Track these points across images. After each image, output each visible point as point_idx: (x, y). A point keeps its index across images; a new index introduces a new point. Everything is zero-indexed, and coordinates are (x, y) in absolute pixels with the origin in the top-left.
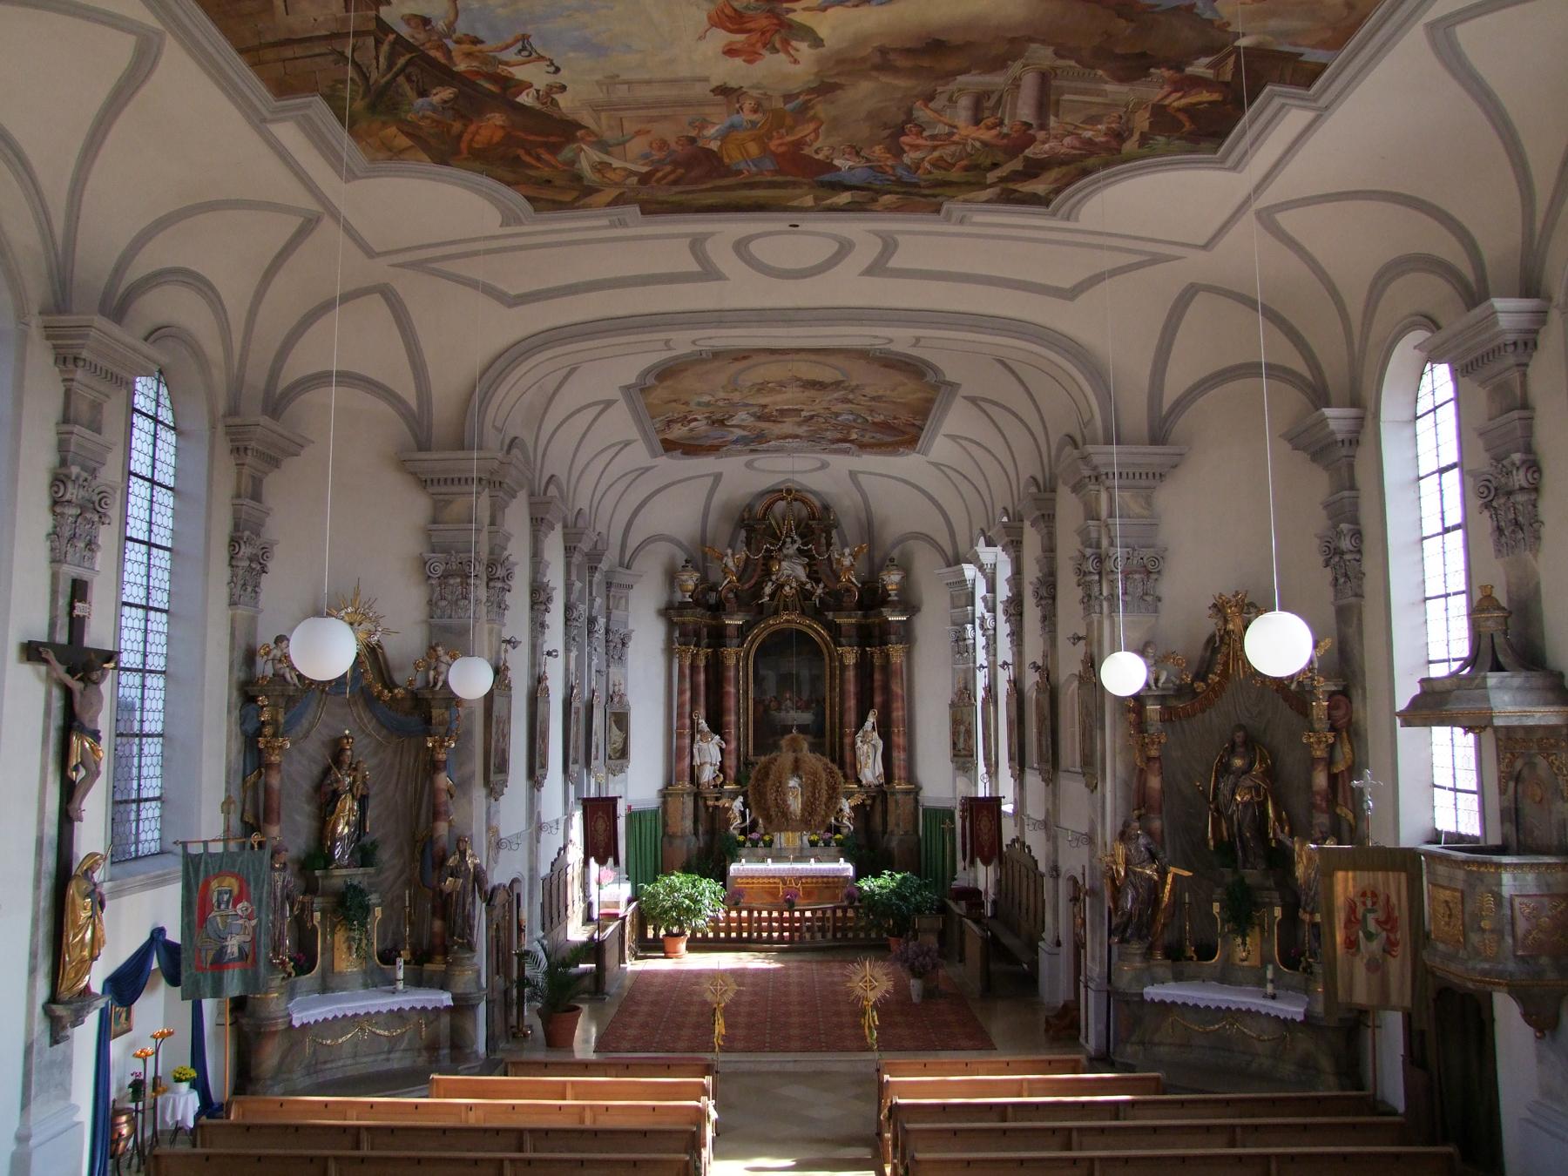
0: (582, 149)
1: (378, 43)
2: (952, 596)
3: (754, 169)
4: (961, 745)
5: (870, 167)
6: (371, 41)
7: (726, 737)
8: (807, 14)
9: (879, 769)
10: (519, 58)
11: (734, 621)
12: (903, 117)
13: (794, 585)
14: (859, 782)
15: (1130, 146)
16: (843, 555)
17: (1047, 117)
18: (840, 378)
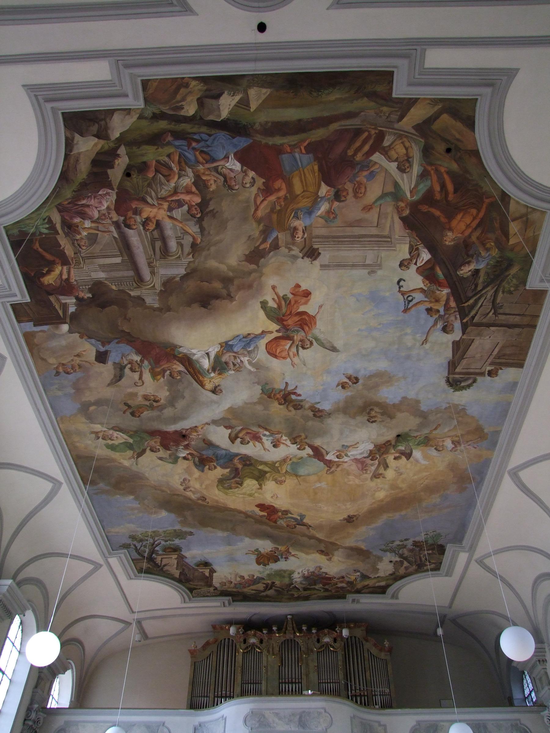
0: (411, 192)
1: (473, 318)
3: (297, 155)
5: (214, 160)
6: (476, 320)
8: (270, 330)
10: (414, 295)
12: (205, 224)
15: (57, 218)
17: (119, 236)
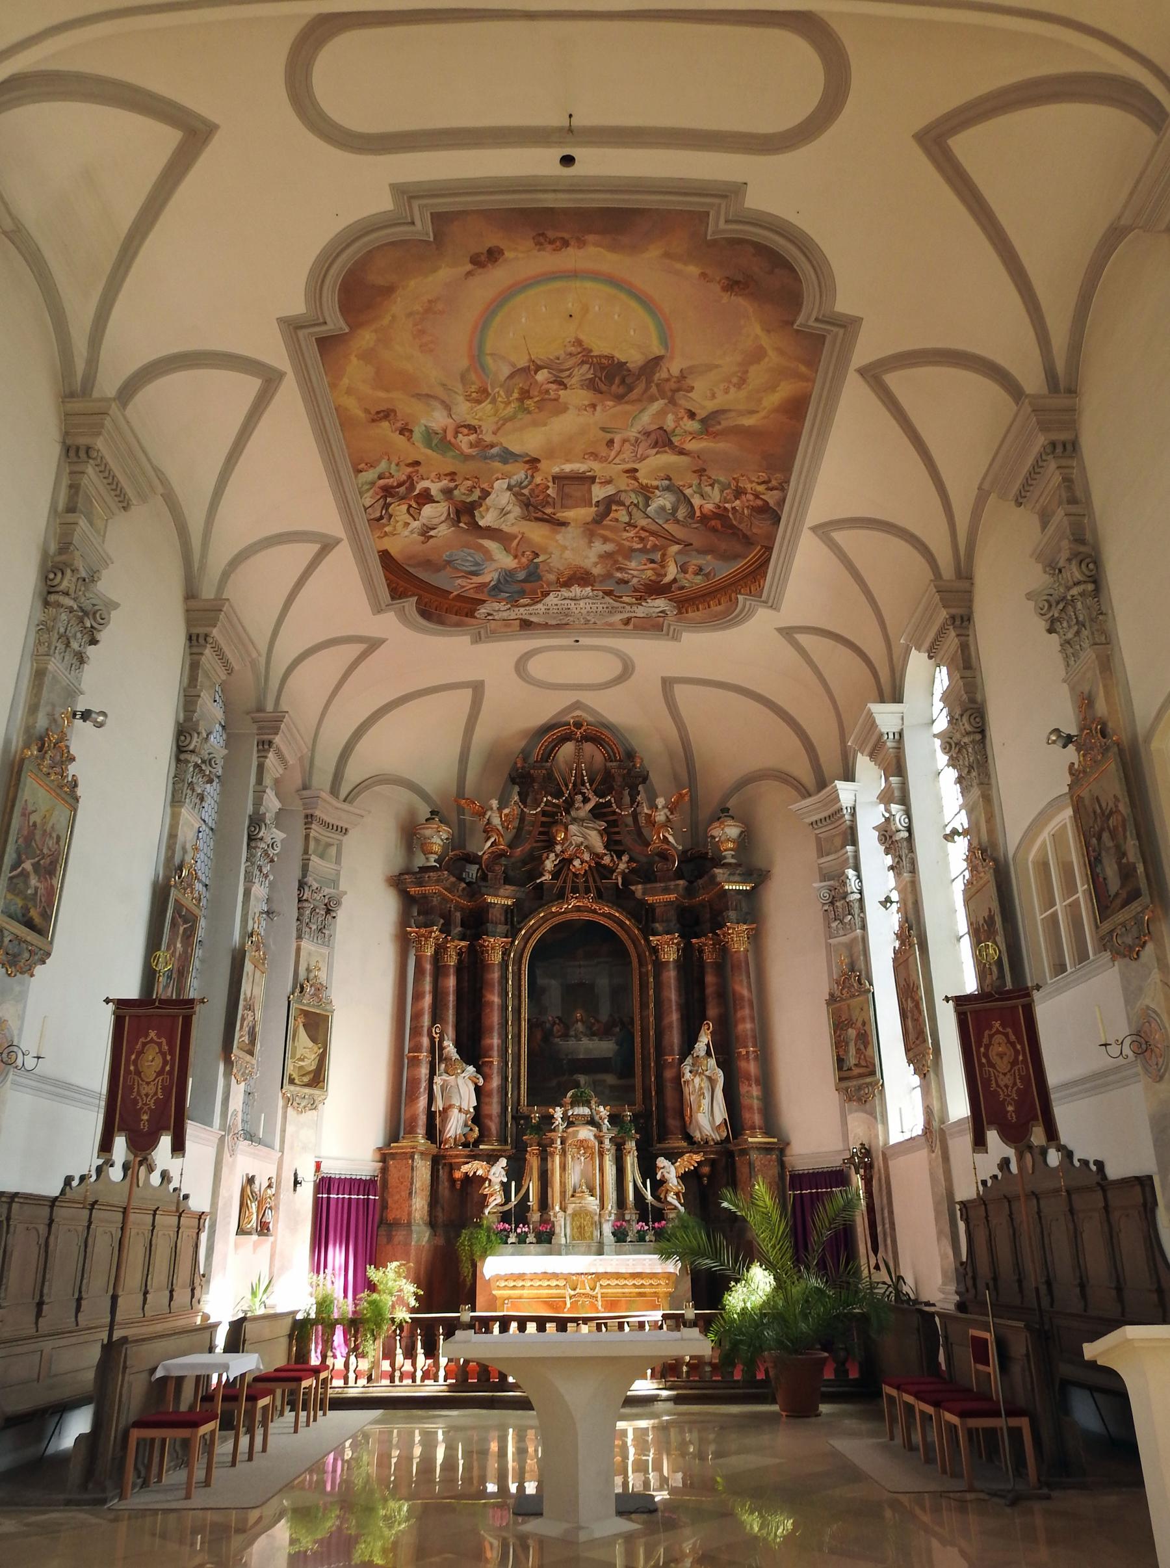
2: (818, 840)
4: (852, 1060)
7: (486, 1069)
9: (721, 1114)
11: (500, 899)
13: (586, 857)
14: (689, 1138)
16: (653, 806)
18: (657, 350)
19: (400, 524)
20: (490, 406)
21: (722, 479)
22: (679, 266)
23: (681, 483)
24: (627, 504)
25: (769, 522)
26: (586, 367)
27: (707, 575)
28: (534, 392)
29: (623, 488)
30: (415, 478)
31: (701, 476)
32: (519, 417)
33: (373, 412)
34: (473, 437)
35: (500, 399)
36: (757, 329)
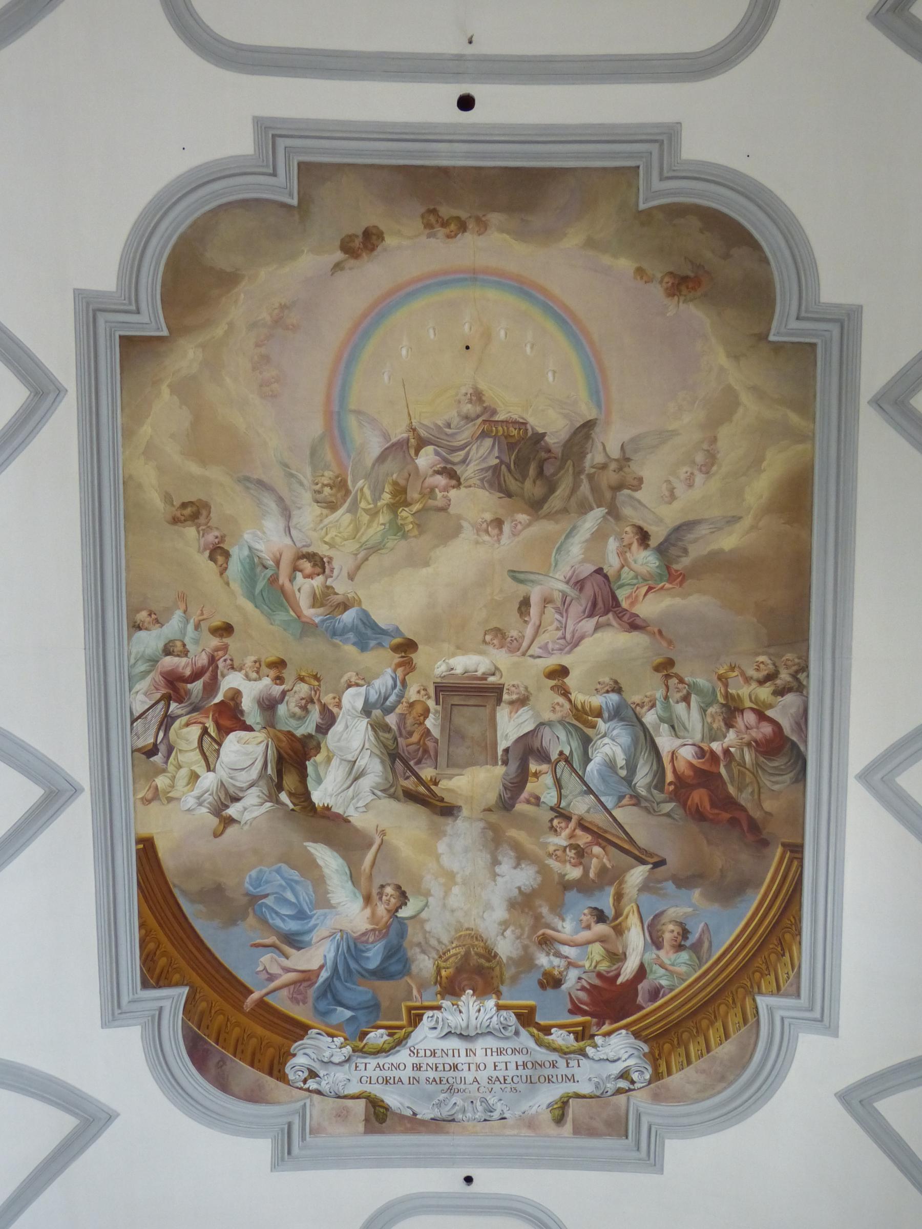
18: (587, 411)
19: (184, 773)
20: (348, 517)
21: (701, 681)
22: (606, 260)
23: (637, 699)
24: (554, 756)
25: (788, 778)
26: (488, 442)
27: (696, 948)
28: (413, 494)
29: (547, 716)
30: (221, 664)
31: (668, 677)
32: (390, 545)
33: (177, 503)
34: (318, 582)
35: (363, 505)
36: (722, 359)
